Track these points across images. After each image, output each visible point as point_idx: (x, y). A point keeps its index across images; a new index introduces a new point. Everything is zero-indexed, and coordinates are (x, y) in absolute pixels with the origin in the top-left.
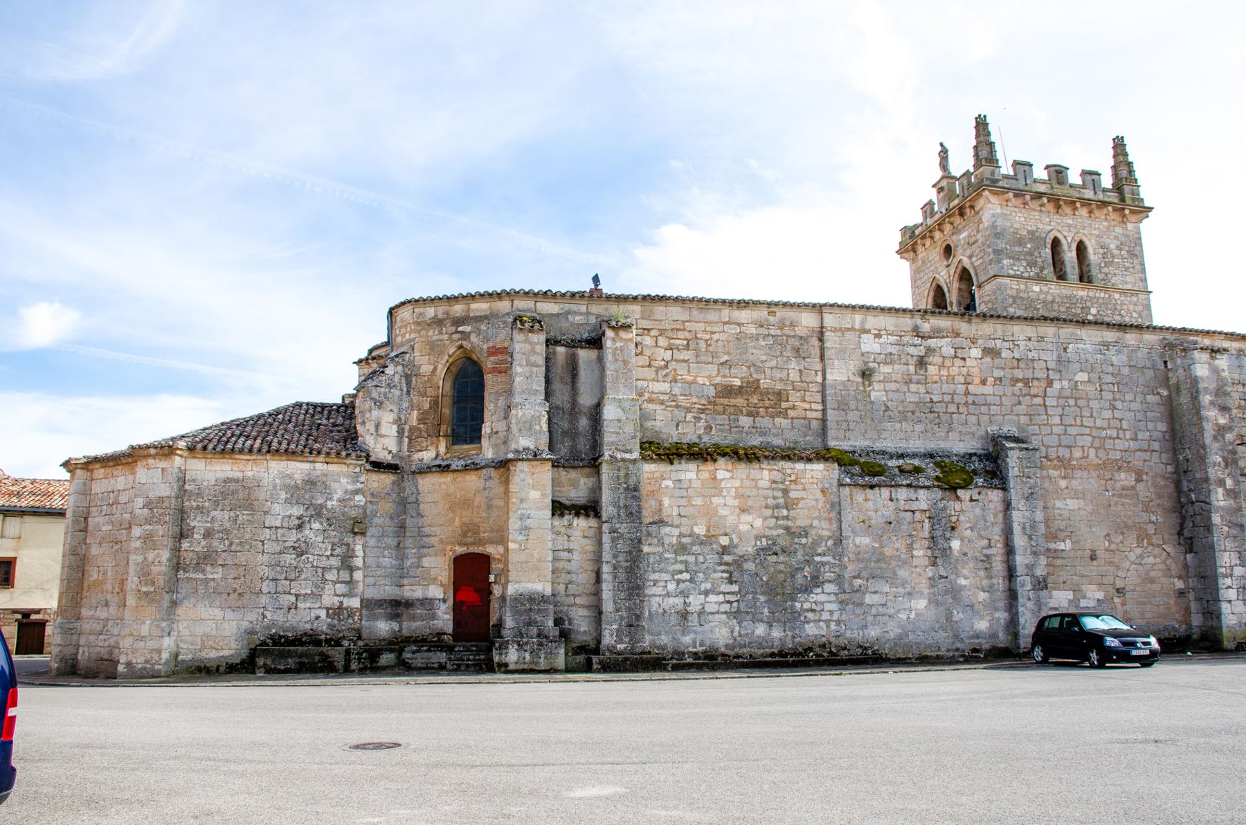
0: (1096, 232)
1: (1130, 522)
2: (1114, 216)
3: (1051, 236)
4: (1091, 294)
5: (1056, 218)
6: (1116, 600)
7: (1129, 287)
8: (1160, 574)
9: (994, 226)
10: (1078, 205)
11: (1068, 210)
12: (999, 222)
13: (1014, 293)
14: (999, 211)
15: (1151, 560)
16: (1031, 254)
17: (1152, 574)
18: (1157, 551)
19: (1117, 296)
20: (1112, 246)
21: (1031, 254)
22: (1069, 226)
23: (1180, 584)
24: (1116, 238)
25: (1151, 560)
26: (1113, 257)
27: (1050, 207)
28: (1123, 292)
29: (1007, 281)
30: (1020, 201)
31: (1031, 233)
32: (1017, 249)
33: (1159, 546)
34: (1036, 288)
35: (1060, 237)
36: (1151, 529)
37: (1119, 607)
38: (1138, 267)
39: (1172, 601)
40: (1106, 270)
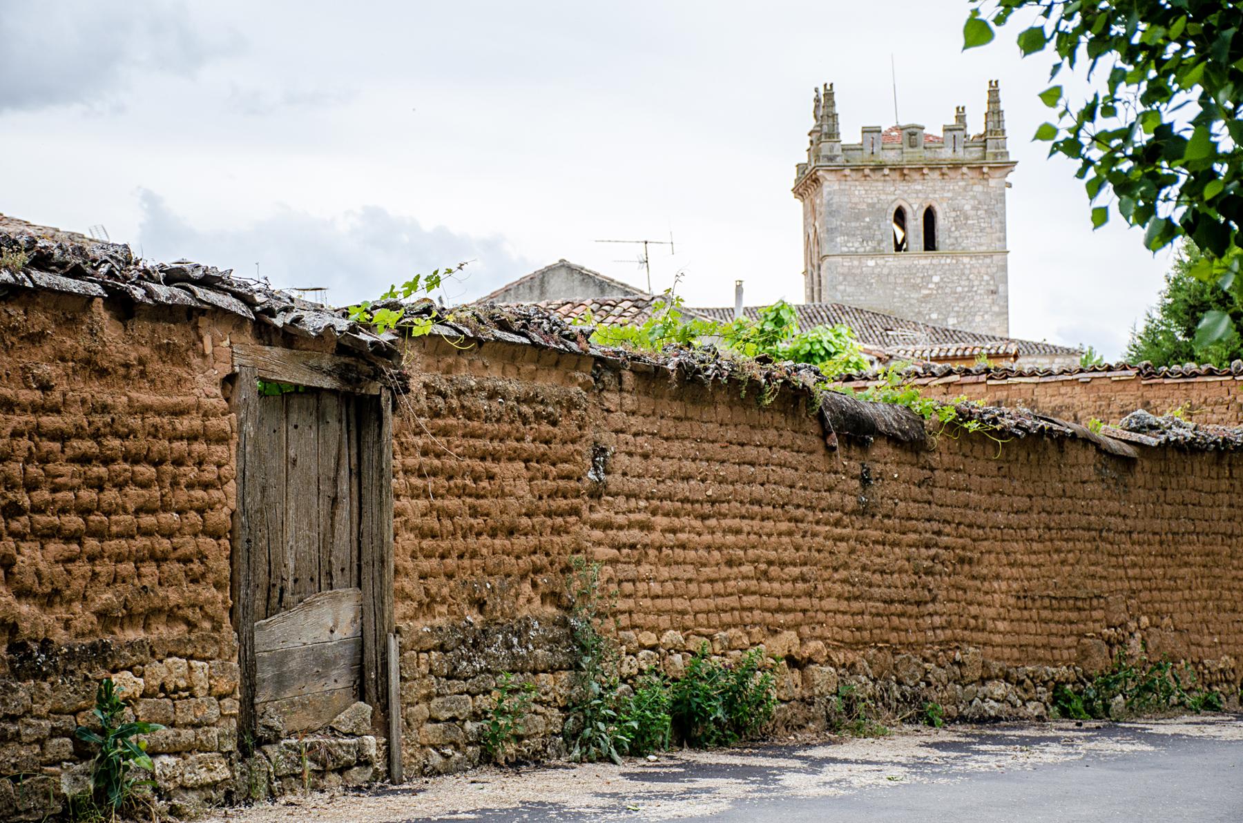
0: (950, 195)
2: (971, 174)
3: (895, 207)
4: (935, 261)
5: (902, 186)
7: (984, 248)
9: (829, 204)
10: (925, 171)
11: (916, 176)
12: (836, 199)
13: (846, 270)
14: (836, 187)
16: (869, 228)
19: (966, 260)
20: (967, 207)
21: (869, 228)
22: (917, 192)
24: (974, 197)
26: (967, 218)
27: (896, 175)
28: (973, 255)
29: (840, 259)
30: (860, 174)
31: (872, 205)
32: (853, 224)
34: (871, 263)
35: (905, 205)
38: (998, 226)
40: (957, 234)
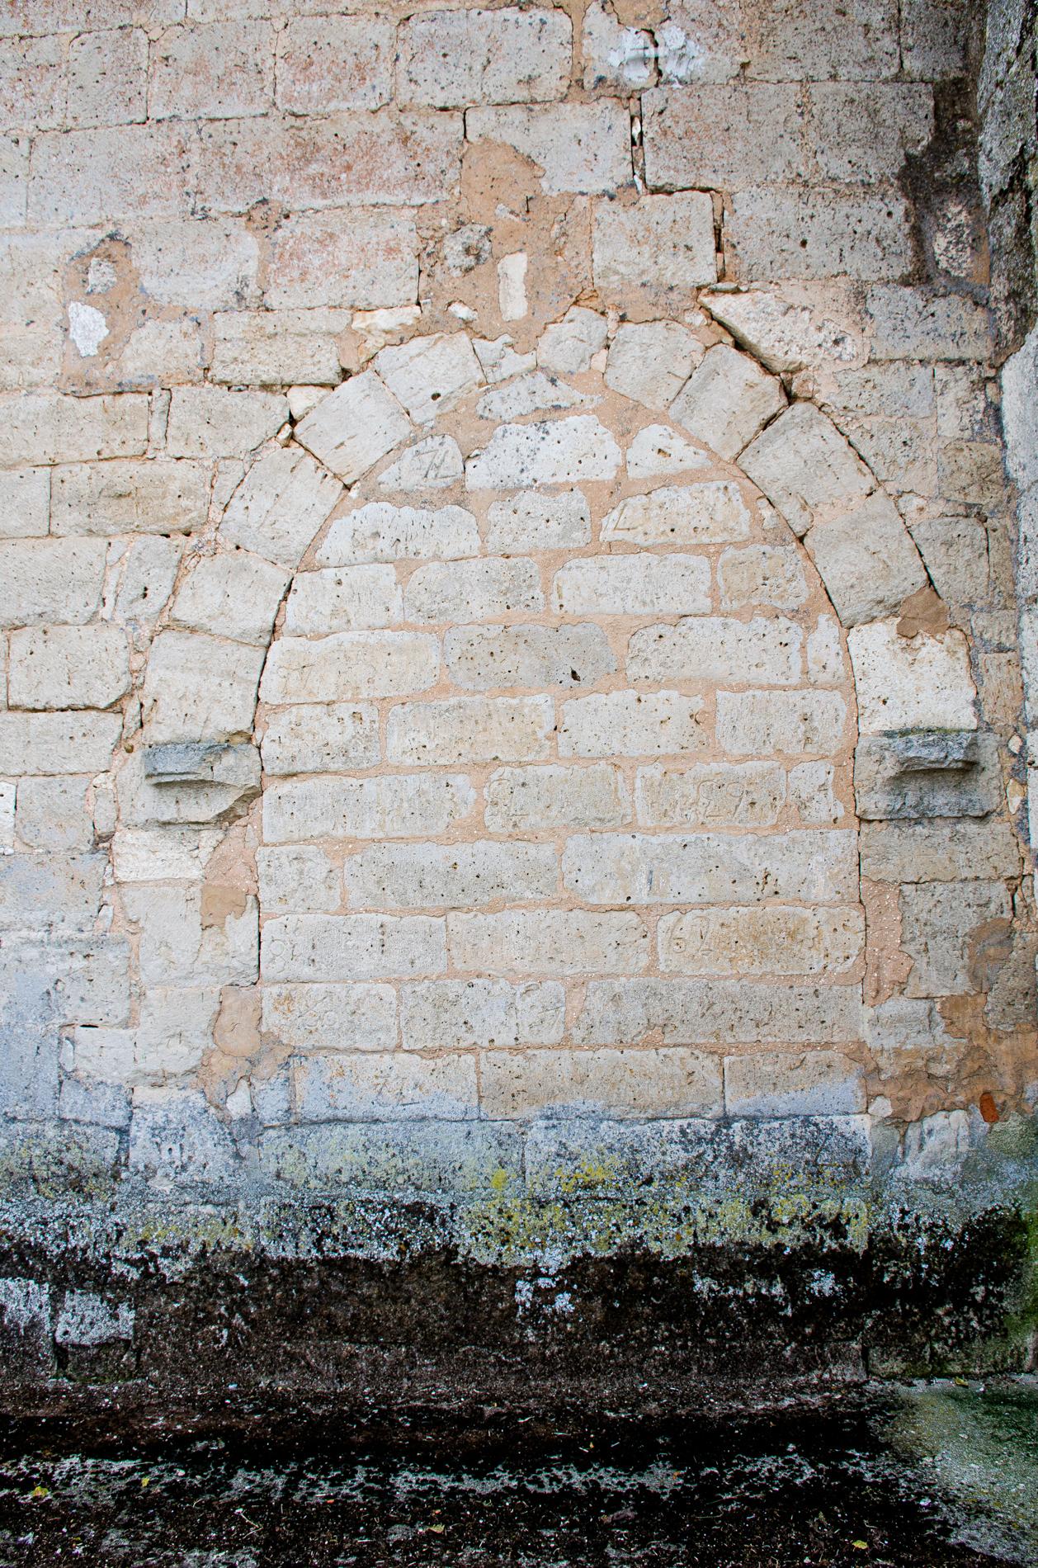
1: (352, 114)
6: (142, 858)
8: (684, 584)
15: (578, 447)
17: (585, 586)
18: (649, 354)
23: (927, 689)
25: (578, 447)
33: (665, 304)
36: (580, 151)
37: (174, 927)
39: (818, 865)
